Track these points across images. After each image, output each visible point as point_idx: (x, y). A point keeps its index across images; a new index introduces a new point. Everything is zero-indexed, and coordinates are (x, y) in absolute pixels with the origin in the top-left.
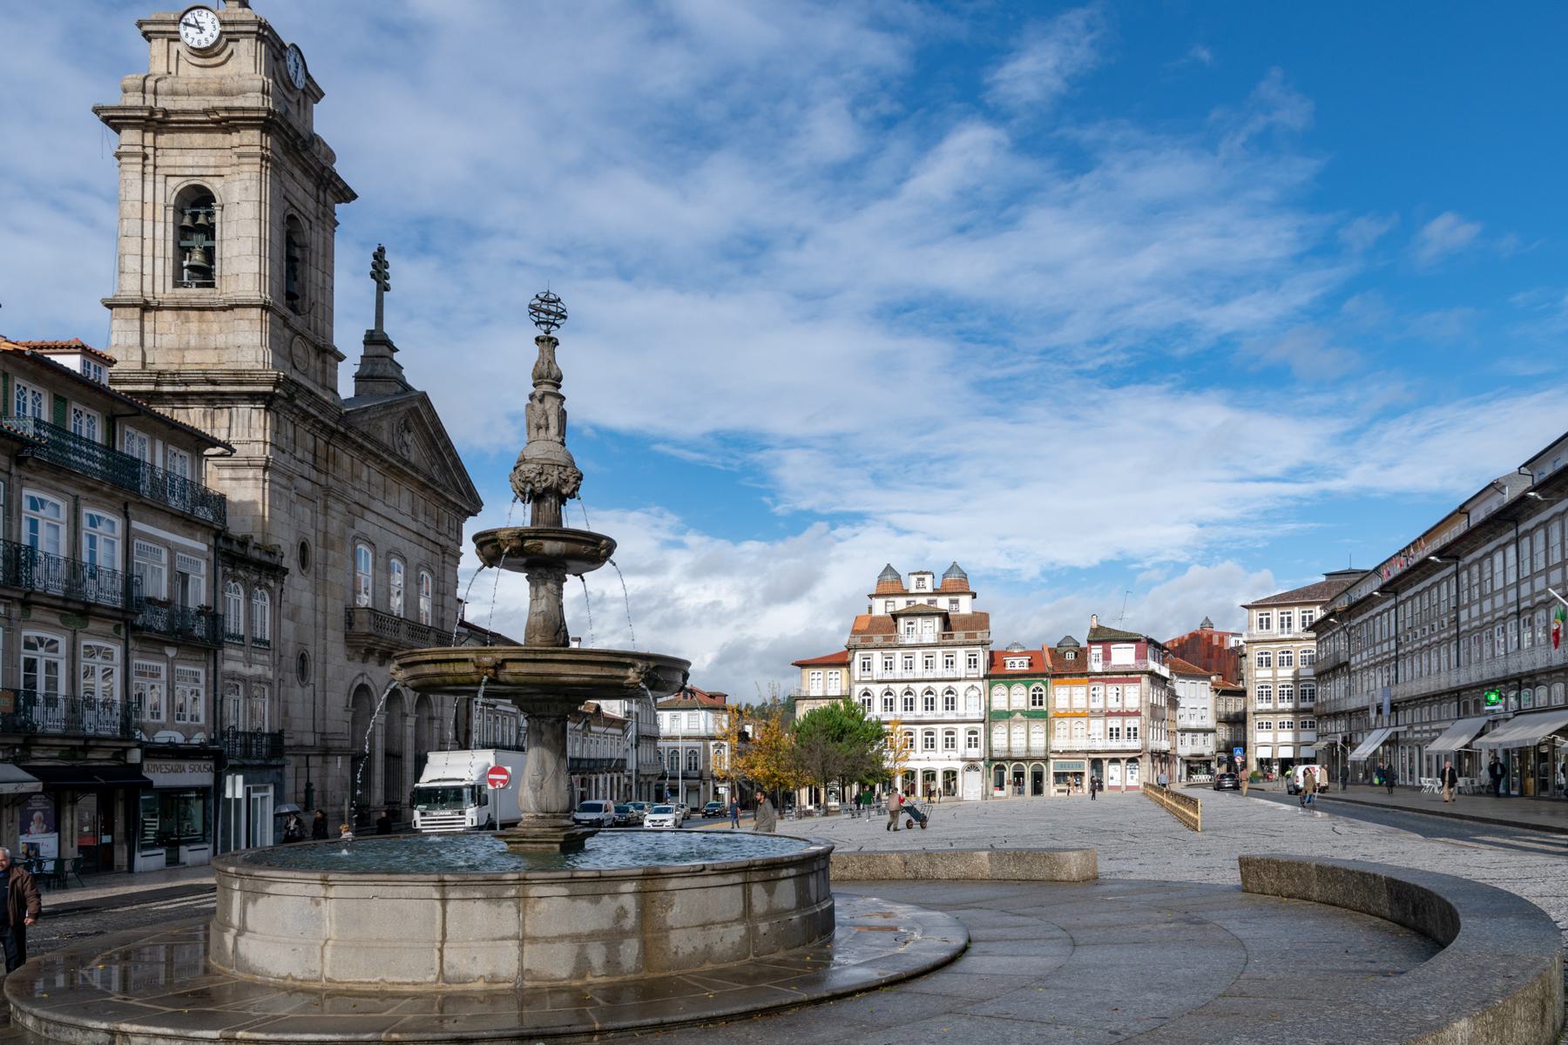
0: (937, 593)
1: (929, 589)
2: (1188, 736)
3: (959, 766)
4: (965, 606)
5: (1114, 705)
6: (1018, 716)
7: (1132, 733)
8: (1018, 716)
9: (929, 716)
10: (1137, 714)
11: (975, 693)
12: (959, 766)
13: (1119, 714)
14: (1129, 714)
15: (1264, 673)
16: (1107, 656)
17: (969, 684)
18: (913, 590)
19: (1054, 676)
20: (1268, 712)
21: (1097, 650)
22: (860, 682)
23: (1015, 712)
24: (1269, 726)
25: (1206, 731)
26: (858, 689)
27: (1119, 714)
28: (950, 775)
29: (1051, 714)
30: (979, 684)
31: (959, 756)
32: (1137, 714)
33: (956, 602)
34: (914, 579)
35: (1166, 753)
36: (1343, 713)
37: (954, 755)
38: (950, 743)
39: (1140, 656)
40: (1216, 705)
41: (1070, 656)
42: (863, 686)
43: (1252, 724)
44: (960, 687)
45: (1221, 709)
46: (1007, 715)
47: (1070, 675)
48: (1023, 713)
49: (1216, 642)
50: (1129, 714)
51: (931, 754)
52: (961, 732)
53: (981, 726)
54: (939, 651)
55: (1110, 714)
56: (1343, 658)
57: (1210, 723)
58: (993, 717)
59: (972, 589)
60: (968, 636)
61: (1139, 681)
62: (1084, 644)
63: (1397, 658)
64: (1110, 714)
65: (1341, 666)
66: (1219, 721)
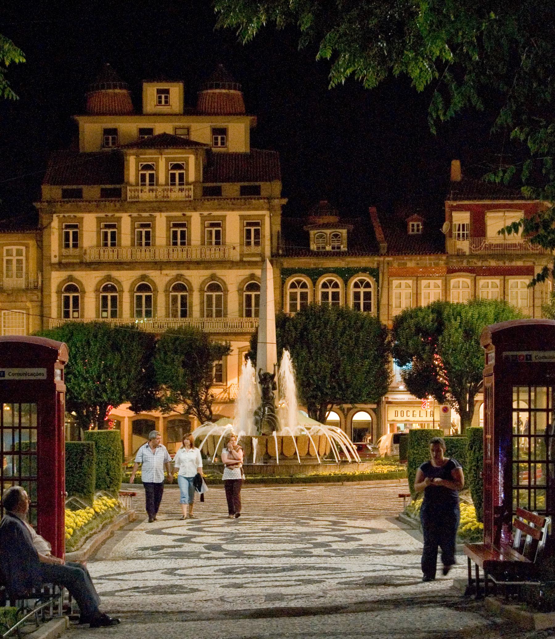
26: (57, 278)
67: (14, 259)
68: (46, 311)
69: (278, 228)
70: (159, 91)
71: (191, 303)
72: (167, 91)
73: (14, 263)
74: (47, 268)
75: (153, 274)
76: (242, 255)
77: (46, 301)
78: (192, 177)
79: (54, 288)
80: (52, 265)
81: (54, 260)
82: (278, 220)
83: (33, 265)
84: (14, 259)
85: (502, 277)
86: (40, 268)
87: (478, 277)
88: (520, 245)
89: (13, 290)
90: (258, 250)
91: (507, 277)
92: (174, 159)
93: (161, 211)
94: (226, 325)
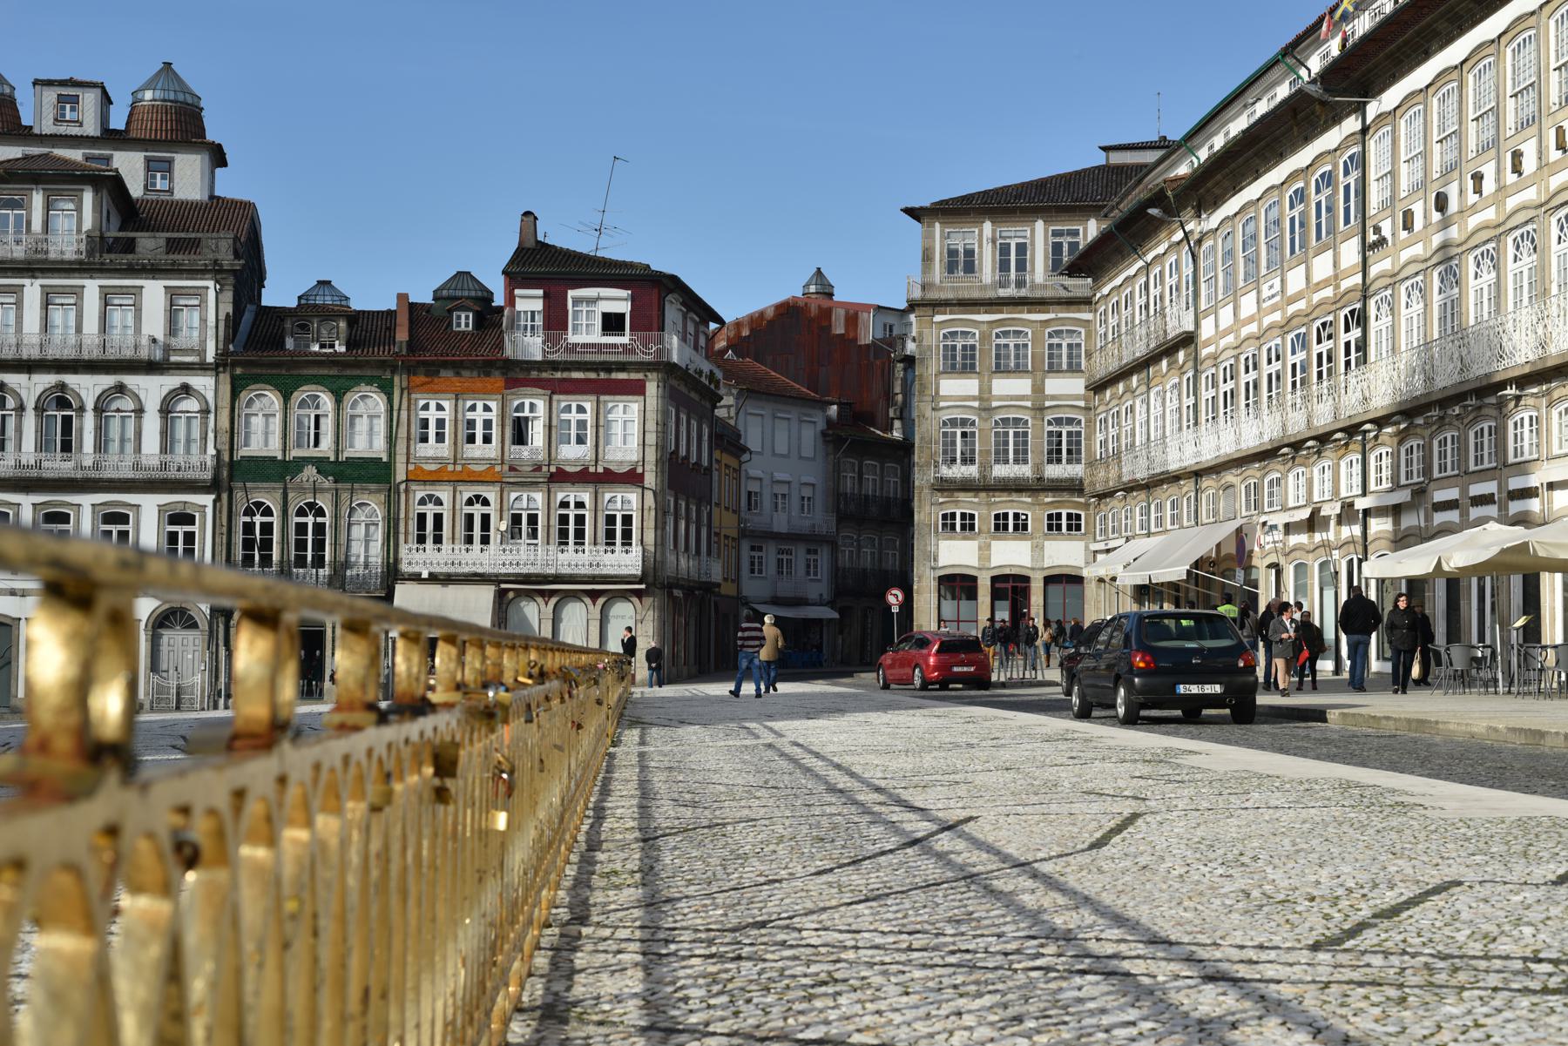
0: (110, 137)
1: (91, 128)
2: (770, 554)
4: (188, 179)
5: (572, 453)
6: (310, 472)
7: (616, 531)
8: (310, 472)
9: (56, 466)
10: (632, 478)
11: (191, 405)
13: (584, 477)
14: (610, 478)
15: (958, 388)
16: (555, 320)
17: (172, 381)
18: (48, 127)
19: (410, 370)
20: (967, 486)
21: (530, 302)
23: (300, 463)
24: (968, 524)
25: (811, 540)
27: (584, 477)
29: (401, 476)
30: (203, 383)
32: (632, 478)
33: (167, 167)
34: (50, 95)
35: (709, 588)
36: (1174, 478)
39: (647, 320)
40: (836, 473)
41: (464, 322)
43: (927, 511)
44: (151, 389)
45: (849, 485)
47: (458, 367)
48: (321, 464)
49: (839, 329)
50: (610, 478)
53: (207, 500)
54: (92, 287)
55: (560, 477)
56: (1179, 321)
57: (820, 519)
59: (211, 136)
60: (173, 246)
61: (637, 389)
62: (496, 285)
63: (1365, 293)
64: (560, 477)
65: (1168, 349)
66: (842, 518)
69: (228, 308)
70: (62, 99)
71: (81, 430)
72: (74, 100)
78: (87, 224)
82: (228, 296)
85: (594, 398)
87: (555, 397)
88: (623, 345)
91: (602, 398)
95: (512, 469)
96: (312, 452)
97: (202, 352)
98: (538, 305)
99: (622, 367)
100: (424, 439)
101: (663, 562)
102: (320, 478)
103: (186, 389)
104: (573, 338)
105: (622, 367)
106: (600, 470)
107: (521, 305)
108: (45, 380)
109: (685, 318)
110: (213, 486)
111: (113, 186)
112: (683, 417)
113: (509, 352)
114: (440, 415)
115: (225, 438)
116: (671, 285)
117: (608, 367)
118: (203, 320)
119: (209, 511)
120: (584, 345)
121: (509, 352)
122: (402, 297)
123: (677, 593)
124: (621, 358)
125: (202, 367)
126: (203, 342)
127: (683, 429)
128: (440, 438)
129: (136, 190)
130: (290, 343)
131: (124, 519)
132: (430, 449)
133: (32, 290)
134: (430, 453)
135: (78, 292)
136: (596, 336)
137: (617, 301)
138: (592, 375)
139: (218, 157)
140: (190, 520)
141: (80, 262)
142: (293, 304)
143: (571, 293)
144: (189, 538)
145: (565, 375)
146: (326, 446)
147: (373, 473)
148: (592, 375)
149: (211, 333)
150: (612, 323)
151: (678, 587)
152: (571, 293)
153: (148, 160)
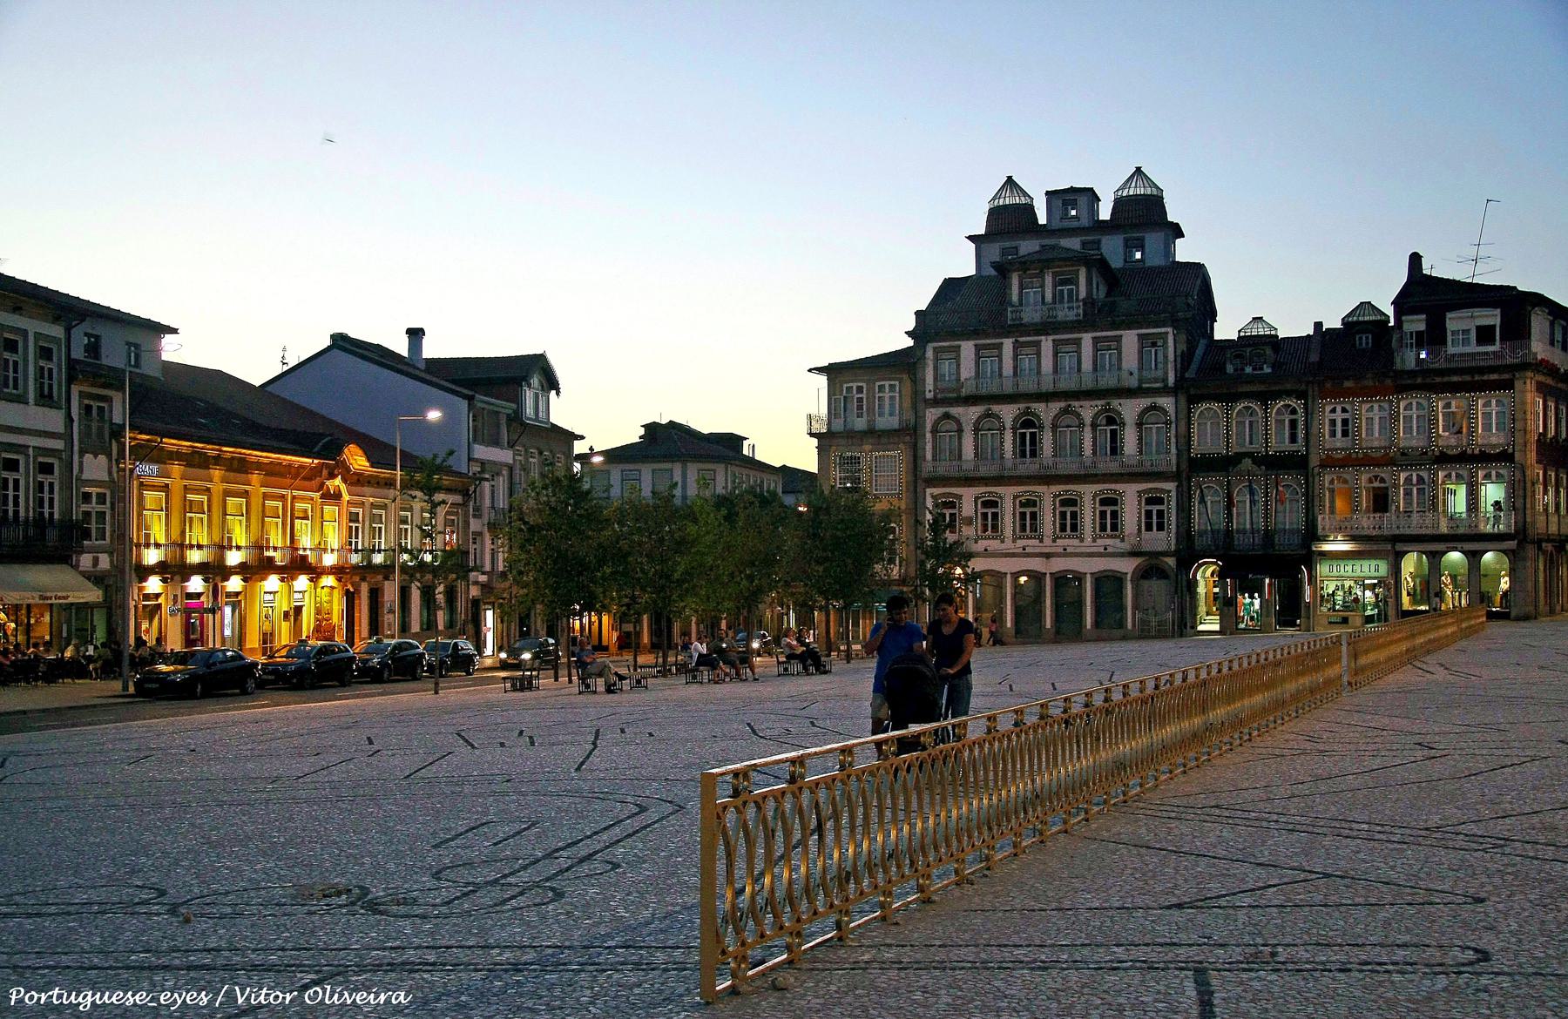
1: (1085, 222)
3: (1127, 566)
6: (1247, 462)
8: (1247, 462)
12: (1127, 566)
16: (1435, 336)
17: (1144, 402)
18: (1056, 224)
21: (1416, 323)
22: (936, 402)
23: (1239, 457)
26: (932, 414)
28: (1108, 584)
29: (1314, 461)
30: (1167, 403)
31: (1124, 547)
37: (1114, 544)
38: (1110, 522)
41: (1365, 341)
42: (940, 411)
44: (1130, 409)
46: (1223, 464)
51: (1072, 544)
52: (1130, 493)
53: (1171, 486)
54: (1087, 339)
58: (1194, 467)
61: (1508, 385)
67: (887, 395)
68: (920, 453)
69: (1183, 347)
73: (887, 401)
74: (921, 406)
75: (1039, 407)
76: (1140, 381)
77: (920, 445)
79: (929, 427)
80: (926, 401)
81: (929, 396)
82: (1183, 337)
83: (907, 404)
84: (887, 395)
86: (915, 407)
89: (883, 431)
90: (1160, 373)
92: (1062, 273)
93: (1048, 334)
94: (1122, 464)
95: (1403, 454)
96: (1248, 448)
97: (1165, 380)
98: (1422, 327)
99: (1492, 369)
100: (1333, 434)
101: (1534, 523)
102: (1255, 468)
103: (1154, 407)
104: (1451, 350)
105: (1492, 369)
106: (1477, 451)
107: (1407, 327)
108: (1056, 407)
109: (1552, 324)
110: (1175, 476)
111: (1102, 266)
112: (1552, 405)
113: (1398, 366)
114: (1346, 416)
115: (1182, 440)
116: (1538, 300)
117: (1481, 370)
118: (1166, 357)
119: (1173, 494)
120: (1461, 355)
121: (1398, 366)
122: (1318, 325)
123: (1548, 547)
124: (1491, 363)
125: (1165, 391)
126: (1166, 373)
127: (1552, 414)
128: (1345, 433)
129: (1116, 262)
130: (1230, 369)
131: (1113, 502)
132: (1340, 441)
133: (1047, 344)
134: (1339, 445)
135: (1078, 342)
136: (1474, 348)
137: (1492, 317)
138: (1467, 378)
139: (1177, 231)
140: (1160, 501)
141: (1079, 322)
142: (1235, 337)
143: (1449, 315)
144: (1160, 514)
145: (1446, 379)
146: (1257, 447)
147: (1295, 463)
148: (1467, 378)
149: (1171, 366)
150: (1485, 335)
151: (1548, 541)
152: (1449, 315)
153: (1126, 241)
